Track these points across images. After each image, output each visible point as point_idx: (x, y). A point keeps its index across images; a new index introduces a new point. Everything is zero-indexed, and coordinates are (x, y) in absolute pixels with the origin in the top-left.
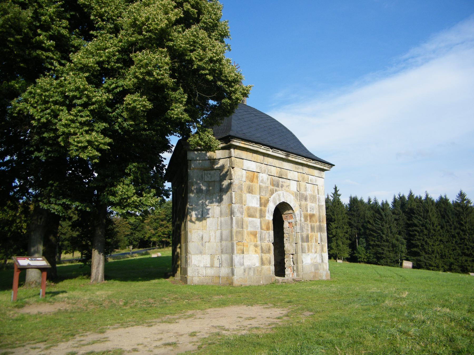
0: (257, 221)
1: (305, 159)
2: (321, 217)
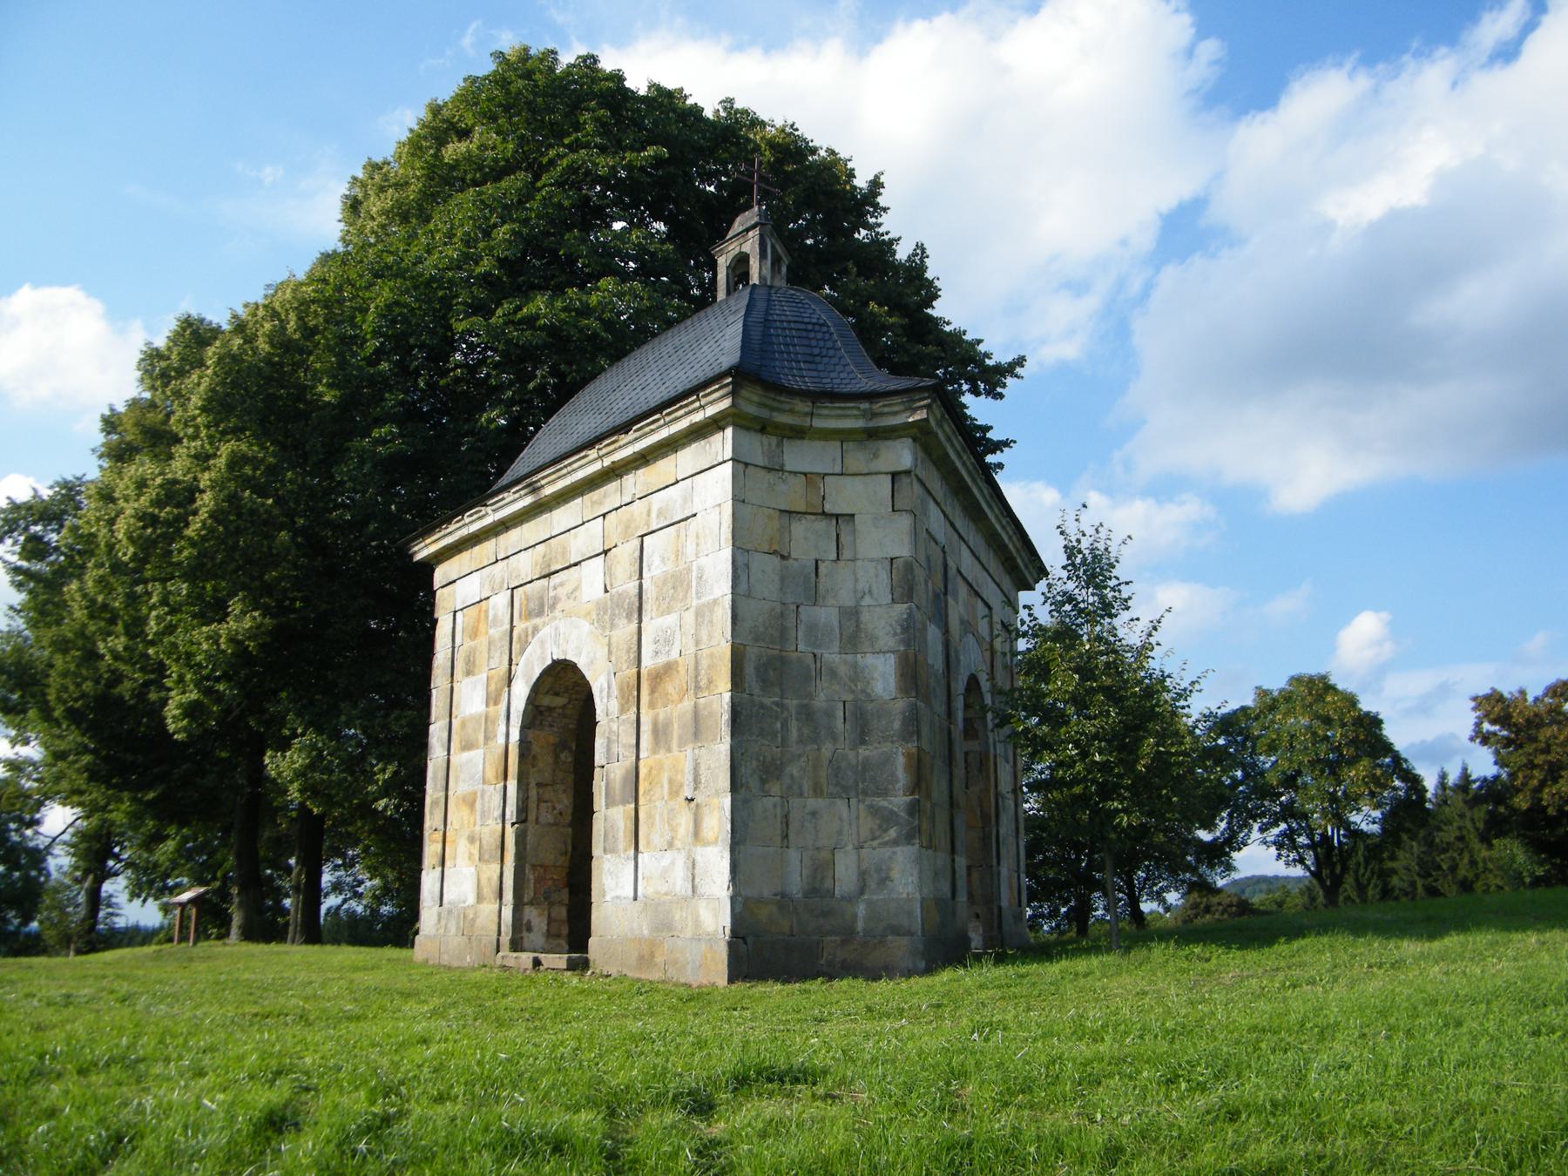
0: (476, 755)
1: (593, 454)
2: (704, 663)
